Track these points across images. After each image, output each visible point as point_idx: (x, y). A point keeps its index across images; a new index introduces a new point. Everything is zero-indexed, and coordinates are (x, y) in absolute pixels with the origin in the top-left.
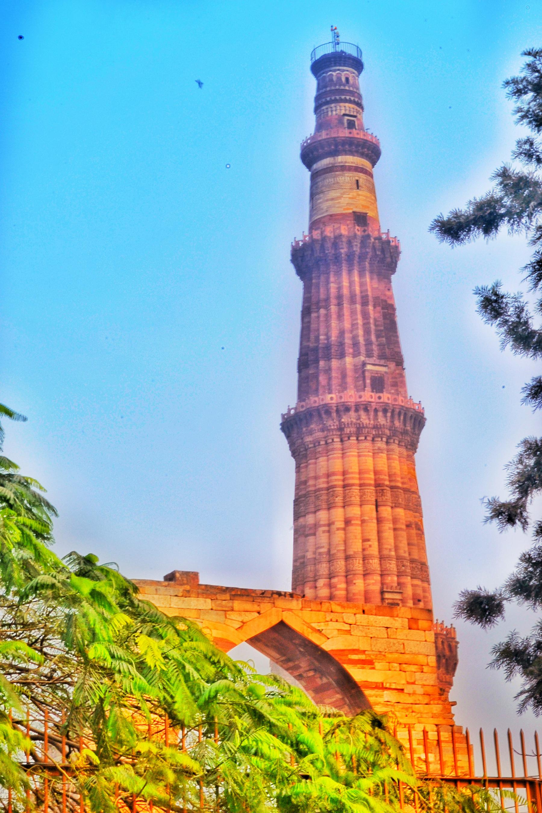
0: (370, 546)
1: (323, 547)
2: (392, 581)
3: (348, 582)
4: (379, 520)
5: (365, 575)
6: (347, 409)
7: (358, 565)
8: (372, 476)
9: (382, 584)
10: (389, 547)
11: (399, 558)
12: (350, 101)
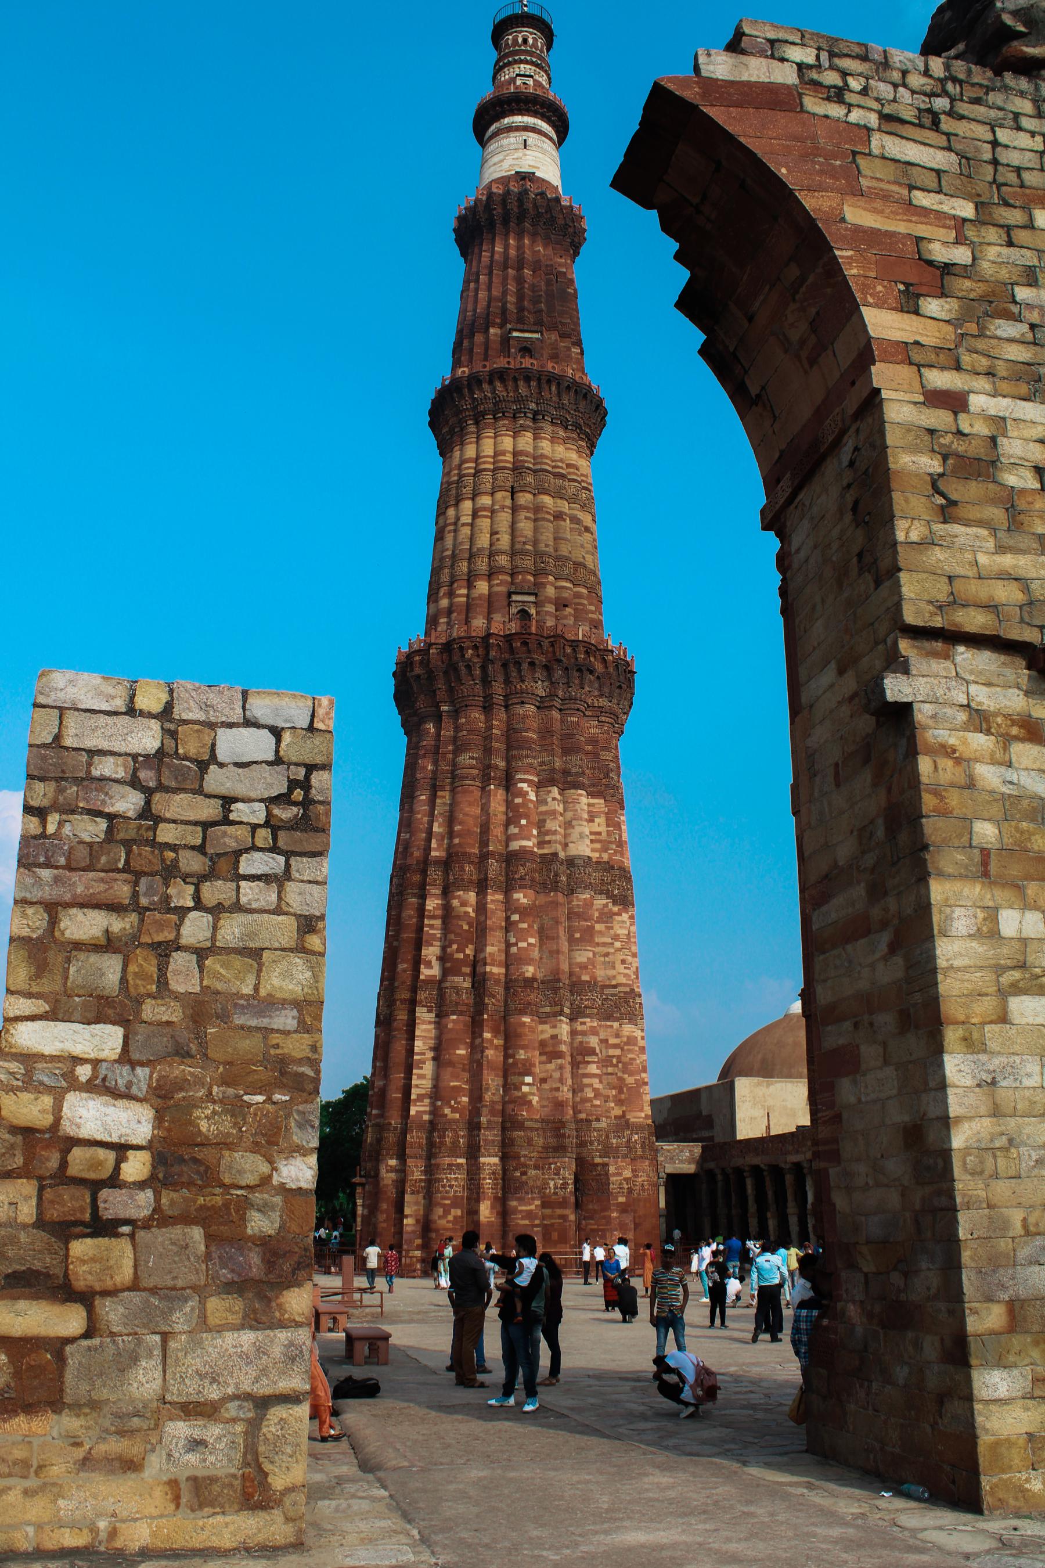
0: (498, 539)
1: (447, 550)
2: (524, 580)
3: (470, 586)
4: (515, 509)
5: (490, 576)
6: (479, 383)
7: (482, 564)
8: (509, 458)
9: (512, 583)
10: (523, 539)
11: (538, 555)
12: (526, 62)
